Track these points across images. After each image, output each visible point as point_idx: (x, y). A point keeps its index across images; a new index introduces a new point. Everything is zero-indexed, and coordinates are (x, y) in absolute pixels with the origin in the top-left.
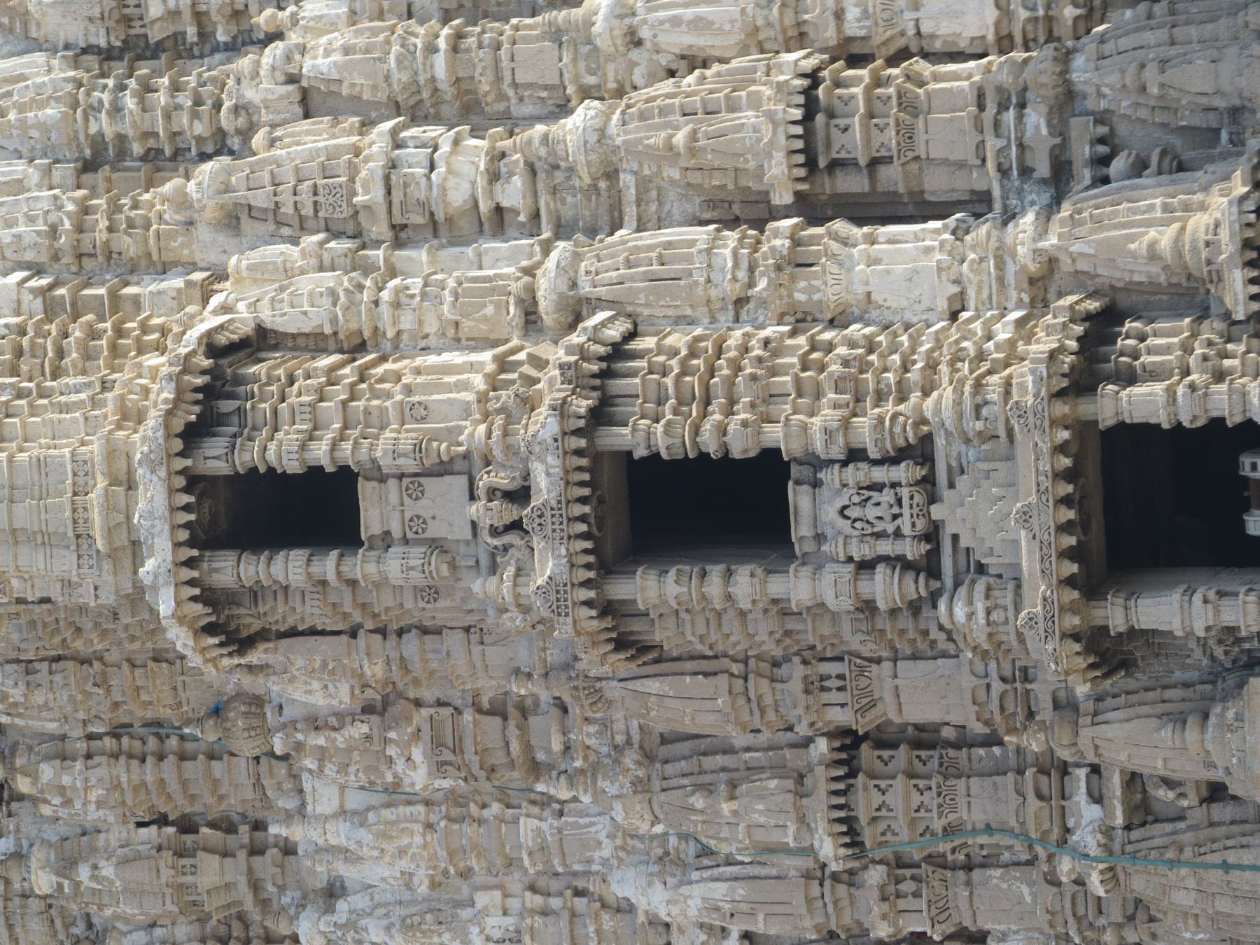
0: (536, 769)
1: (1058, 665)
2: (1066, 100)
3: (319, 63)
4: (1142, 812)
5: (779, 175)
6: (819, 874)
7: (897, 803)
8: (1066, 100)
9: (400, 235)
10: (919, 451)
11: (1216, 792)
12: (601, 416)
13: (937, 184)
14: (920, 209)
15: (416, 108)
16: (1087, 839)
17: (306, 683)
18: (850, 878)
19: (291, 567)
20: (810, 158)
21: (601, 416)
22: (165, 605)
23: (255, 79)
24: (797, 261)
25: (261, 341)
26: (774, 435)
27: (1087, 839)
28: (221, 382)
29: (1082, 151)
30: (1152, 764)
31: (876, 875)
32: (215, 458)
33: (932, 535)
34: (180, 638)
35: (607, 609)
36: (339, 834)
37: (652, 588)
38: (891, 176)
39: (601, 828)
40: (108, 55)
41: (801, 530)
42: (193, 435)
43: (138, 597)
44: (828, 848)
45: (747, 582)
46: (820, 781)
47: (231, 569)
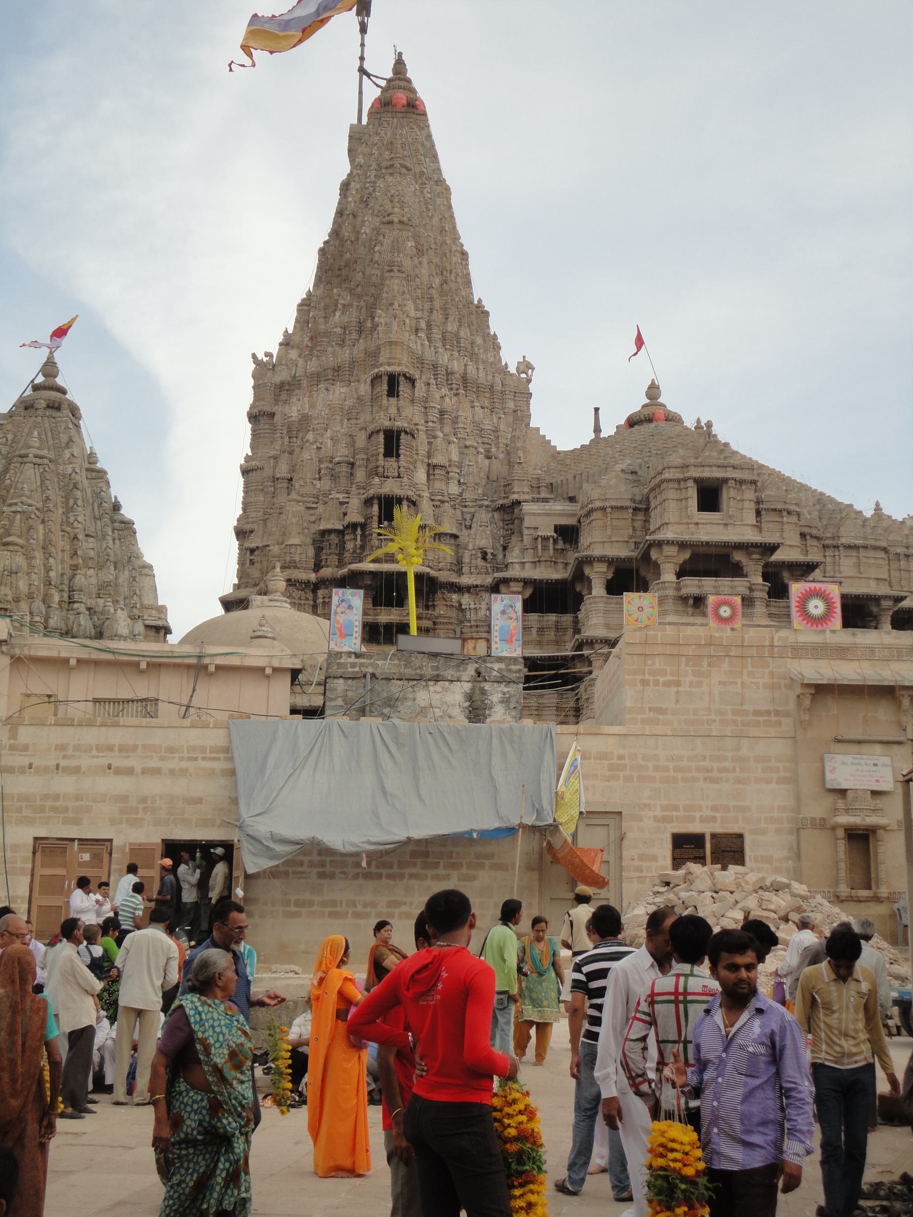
0: (348, 420)
1: (372, 492)
2: (443, 502)
3: (447, 399)
4: (341, 503)
5: (434, 461)
6: (332, 458)
7: (345, 469)
8: (443, 502)
9: (426, 408)
10: (399, 477)
11: (345, 514)
12: (406, 432)
13: (431, 483)
14: (428, 480)
15: (442, 412)
16: (338, 496)
17: (364, 389)
18: (331, 462)
19: (385, 387)
20: (435, 467)
21: (406, 432)
22: (381, 369)
23: (444, 391)
24: (423, 462)
25: (414, 386)
26: (402, 457)
27: (338, 496)
28: (412, 381)
29: (436, 503)
30: (350, 505)
31: (330, 466)
32: (402, 379)
33: (387, 477)
34: (376, 370)
35: (378, 431)
36: (338, 392)
37: (381, 437)
38: (432, 477)
39: (338, 428)
40: (447, 371)
41: (389, 459)
42: (405, 375)
43: (381, 365)
44: (337, 459)
45: (382, 450)
46: (347, 459)
47: (385, 379)
